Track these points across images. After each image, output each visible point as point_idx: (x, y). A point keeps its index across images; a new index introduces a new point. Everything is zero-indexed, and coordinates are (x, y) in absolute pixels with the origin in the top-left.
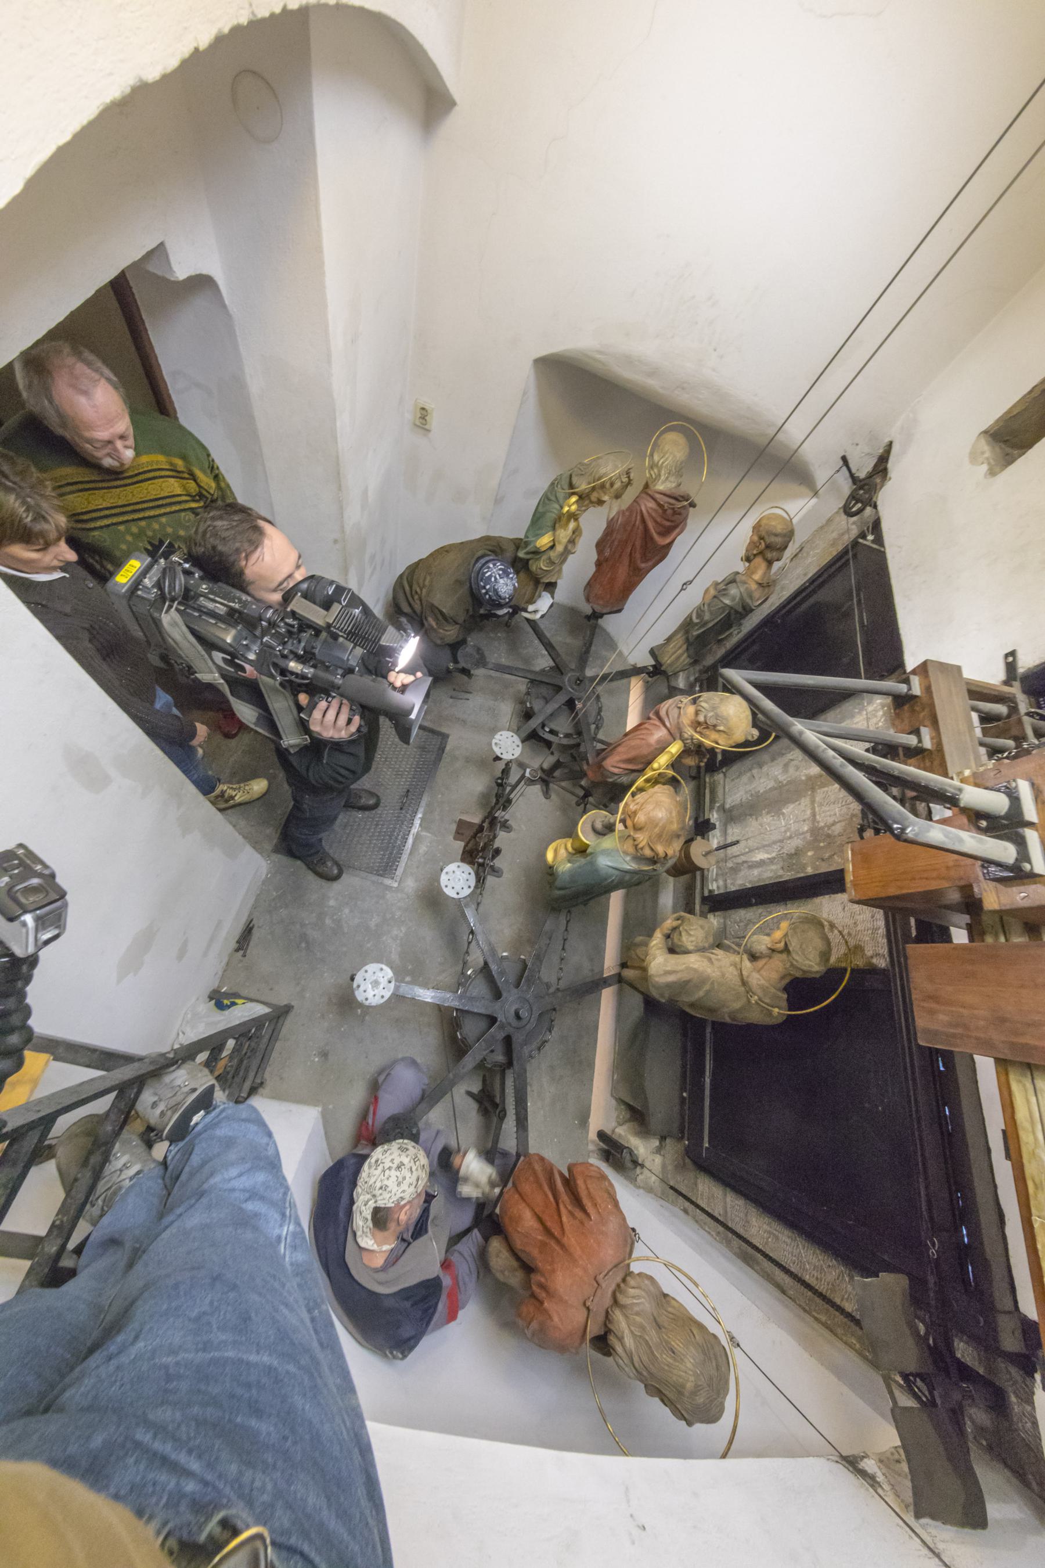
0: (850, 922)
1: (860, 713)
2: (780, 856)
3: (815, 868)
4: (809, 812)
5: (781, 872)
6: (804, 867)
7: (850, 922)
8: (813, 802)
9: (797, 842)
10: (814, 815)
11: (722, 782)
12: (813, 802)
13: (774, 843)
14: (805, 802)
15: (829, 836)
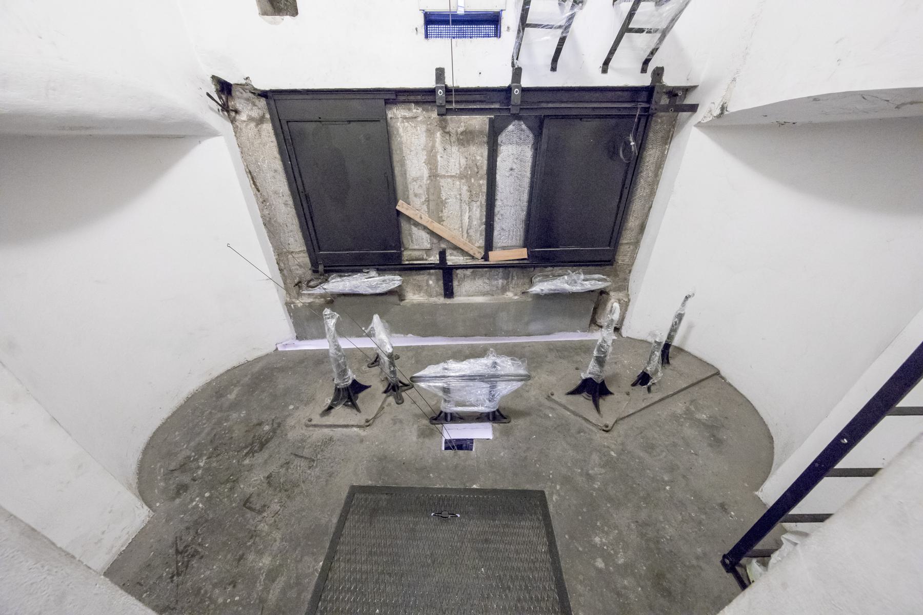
0: (512, 157)
1: (401, 137)
2: (469, 204)
3: (481, 178)
4: (449, 180)
5: (478, 203)
6: (480, 186)
7: (512, 157)
8: (444, 176)
9: (465, 188)
10: (452, 176)
11: (410, 252)
12: (444, 176)
13: (461, 207)
14: (443, 182)
15: (466, 168)
